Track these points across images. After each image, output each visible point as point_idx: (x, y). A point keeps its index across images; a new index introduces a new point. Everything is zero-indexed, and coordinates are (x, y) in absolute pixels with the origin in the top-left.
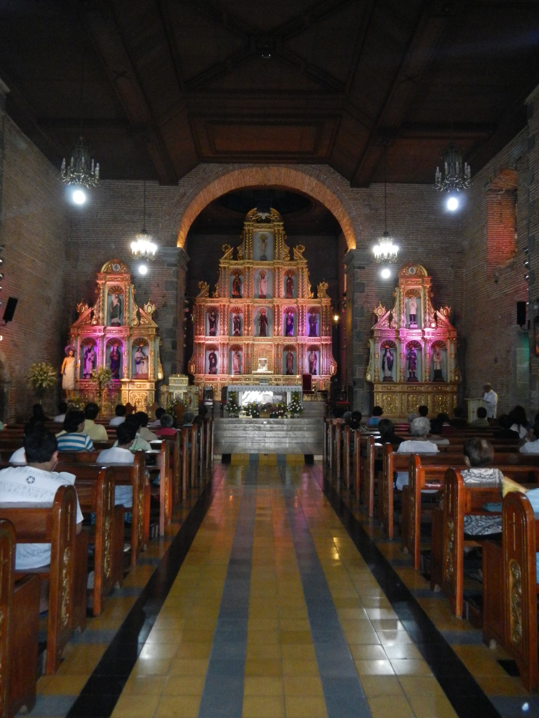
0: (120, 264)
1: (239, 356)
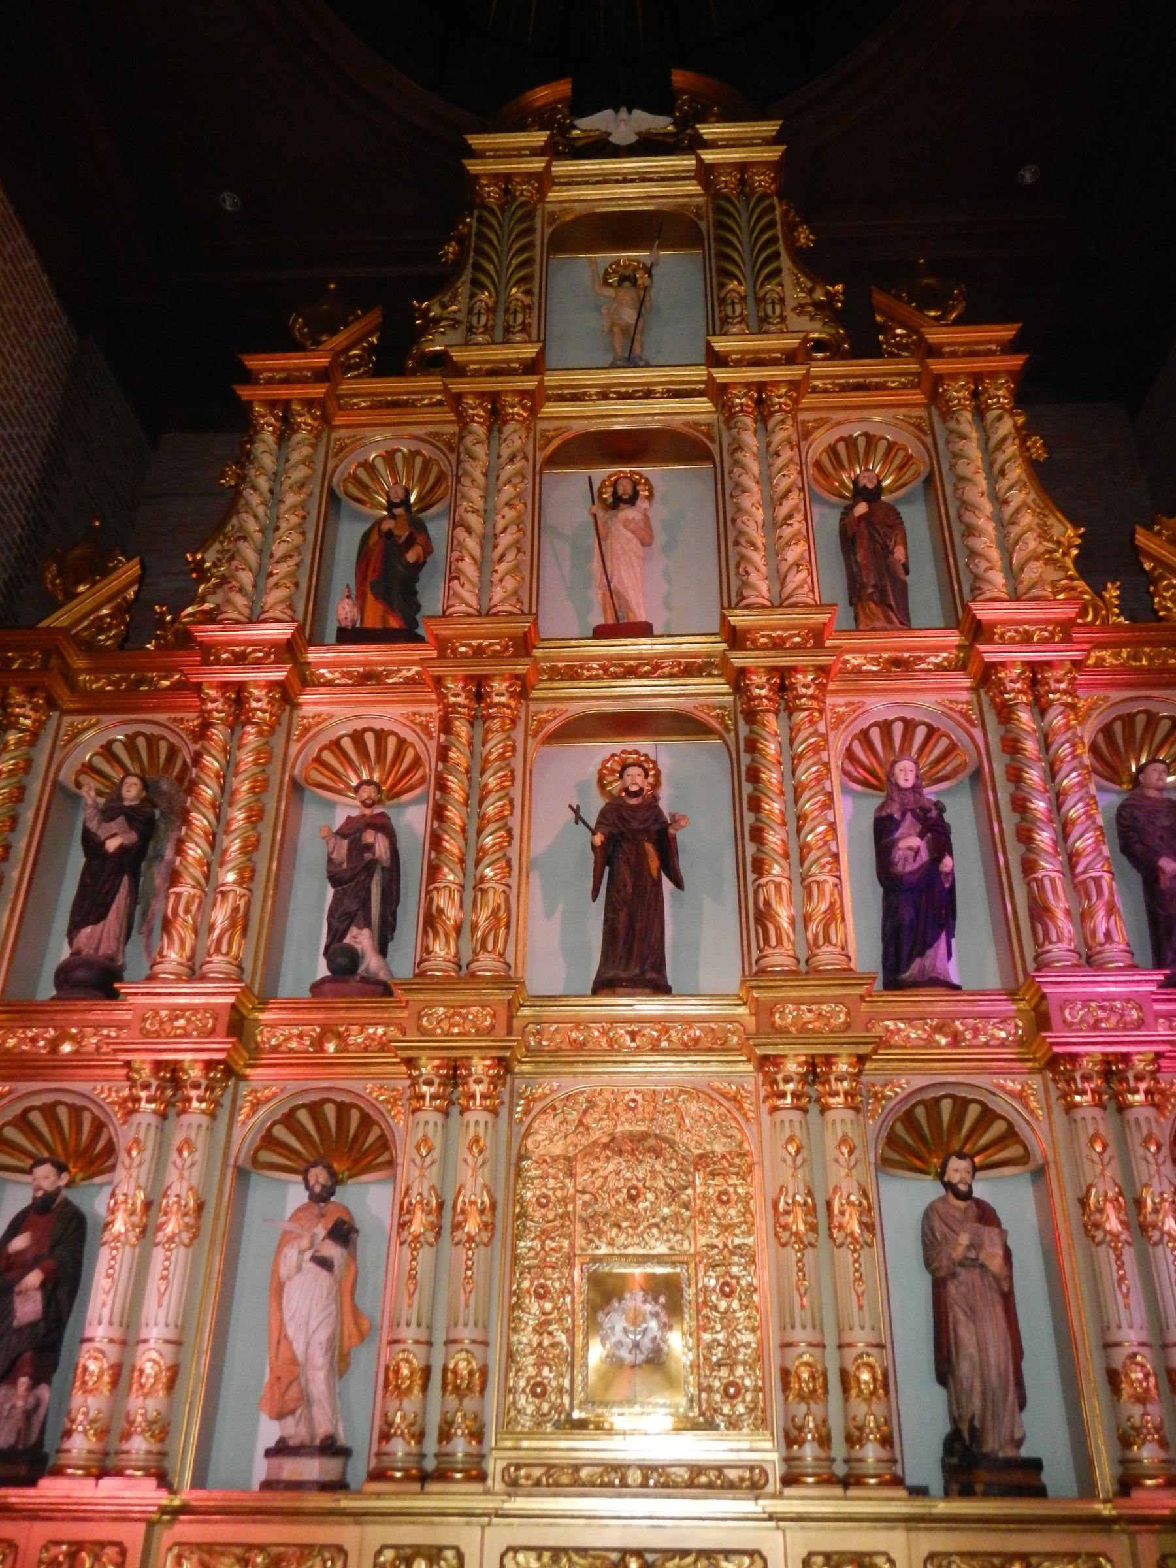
1: (343, 1233)
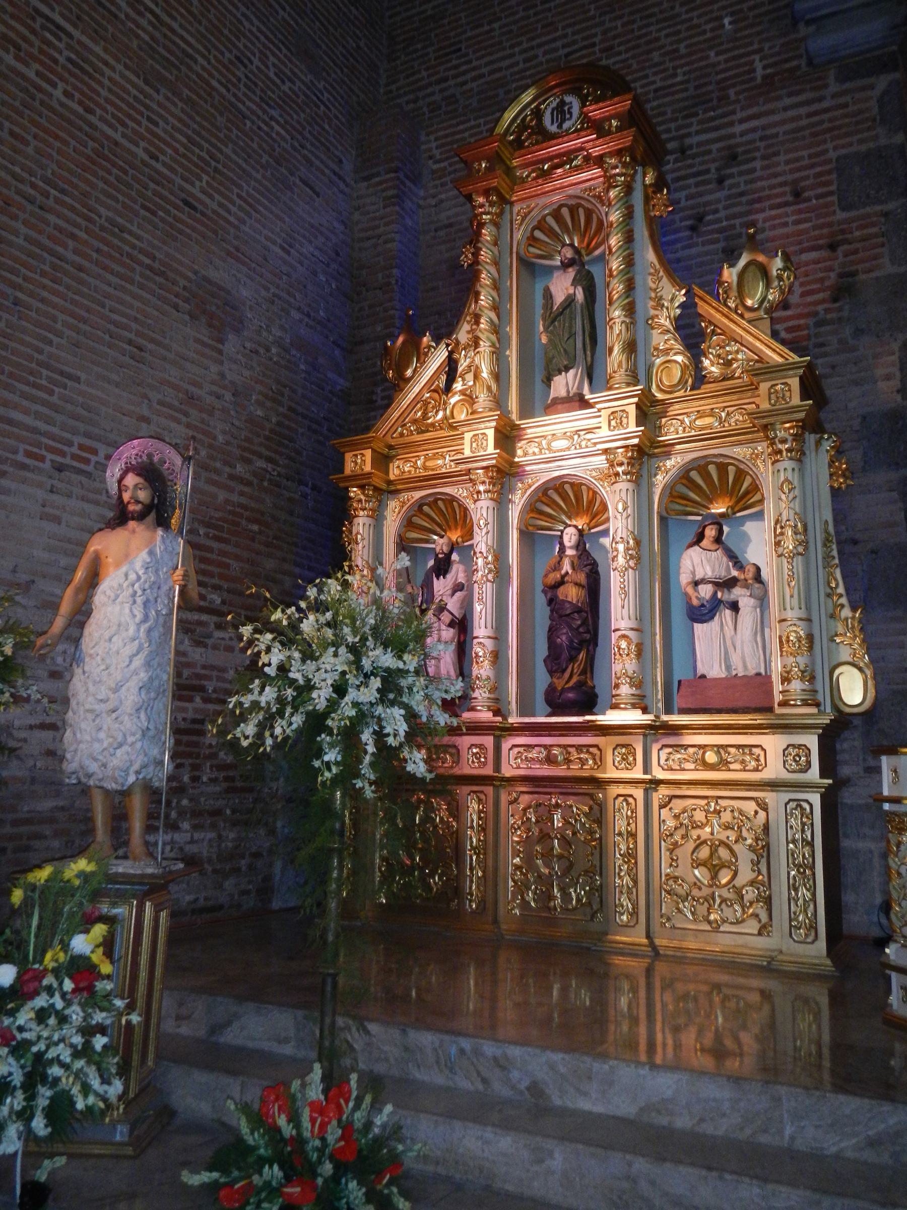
0: (577, 92)
